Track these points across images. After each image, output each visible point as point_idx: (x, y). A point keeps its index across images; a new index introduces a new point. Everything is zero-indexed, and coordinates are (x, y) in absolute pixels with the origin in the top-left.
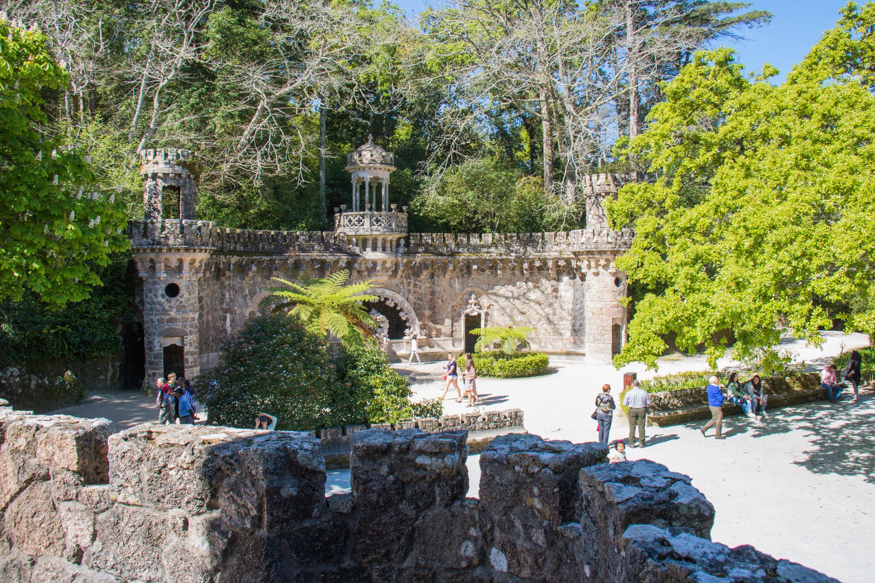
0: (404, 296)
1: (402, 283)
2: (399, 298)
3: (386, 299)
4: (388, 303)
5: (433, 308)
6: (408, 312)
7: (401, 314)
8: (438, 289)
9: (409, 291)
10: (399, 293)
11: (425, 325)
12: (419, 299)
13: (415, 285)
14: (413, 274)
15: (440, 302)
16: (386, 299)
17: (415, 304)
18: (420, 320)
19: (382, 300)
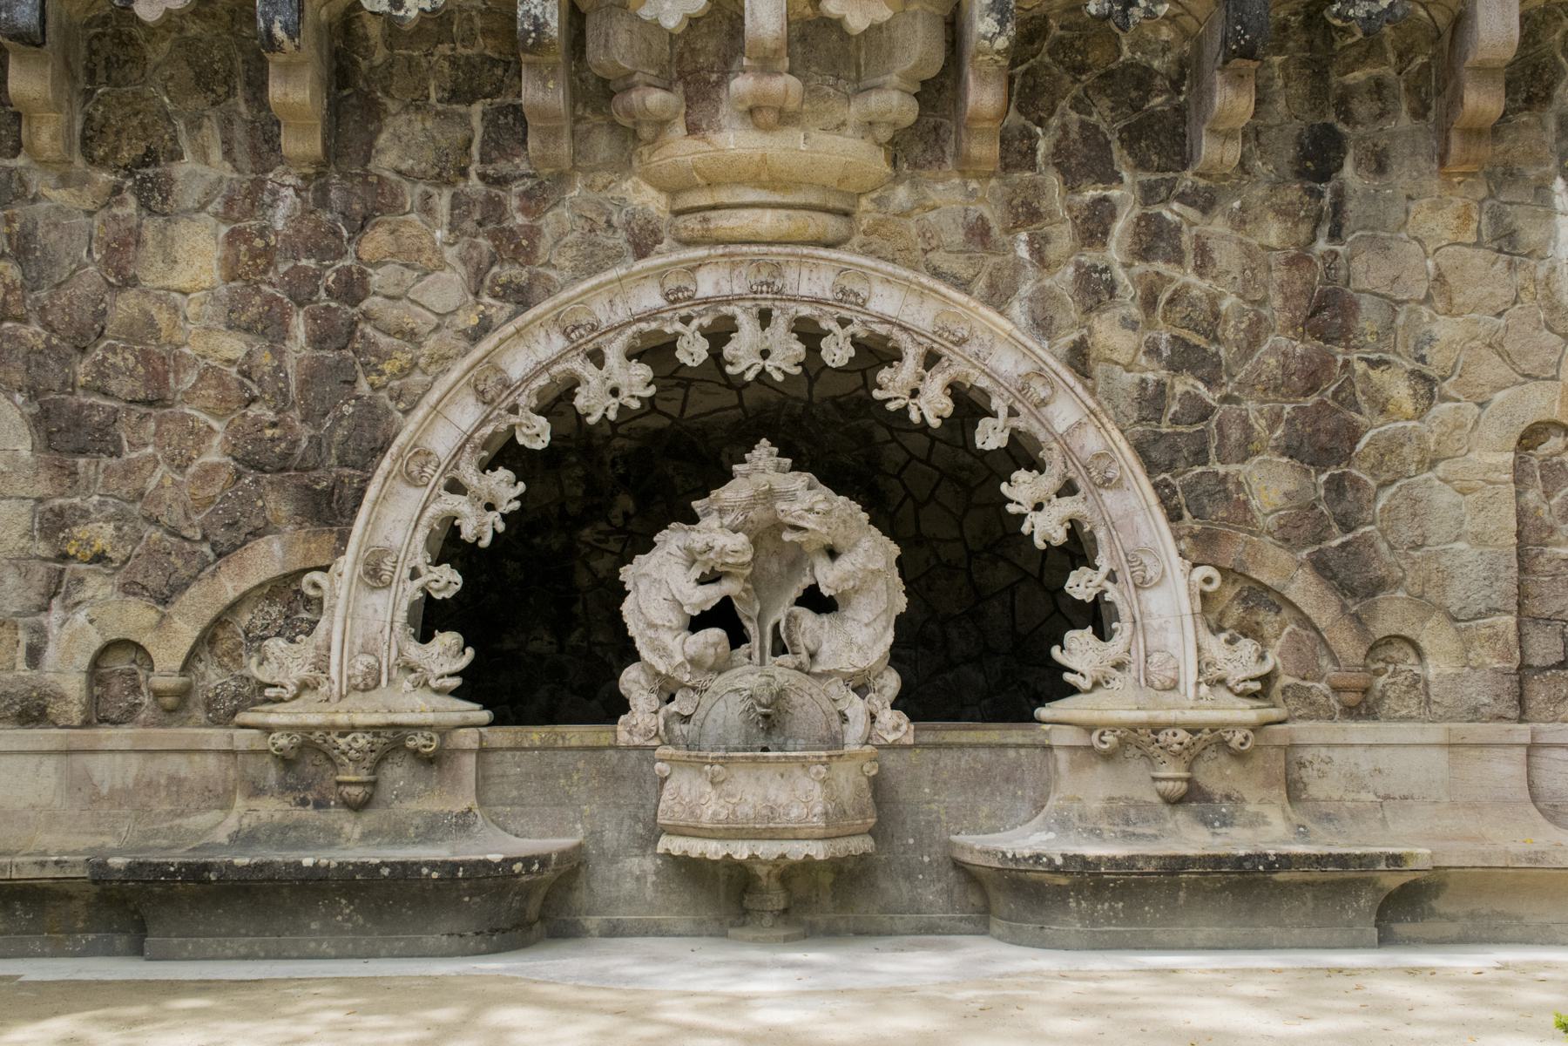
0: (1043, 326)
1: (1028, 214)
2: (1002, 350)
3: (876, 353)
4: (893, 385)
5: (1323, 444)
6: (1087, 483)
7: (1021, 489)
8: (1367, 274)
9: (1096, 289)
10: (998, 297)
11: (1260, 596)
12: (1184, 358)
13: (1153, 239)
14: (1132, 137)
15: (1400, 391)
16: (876, 353)
17: (1153, 400)
18: (1202, 547)
19: (837, 353)
